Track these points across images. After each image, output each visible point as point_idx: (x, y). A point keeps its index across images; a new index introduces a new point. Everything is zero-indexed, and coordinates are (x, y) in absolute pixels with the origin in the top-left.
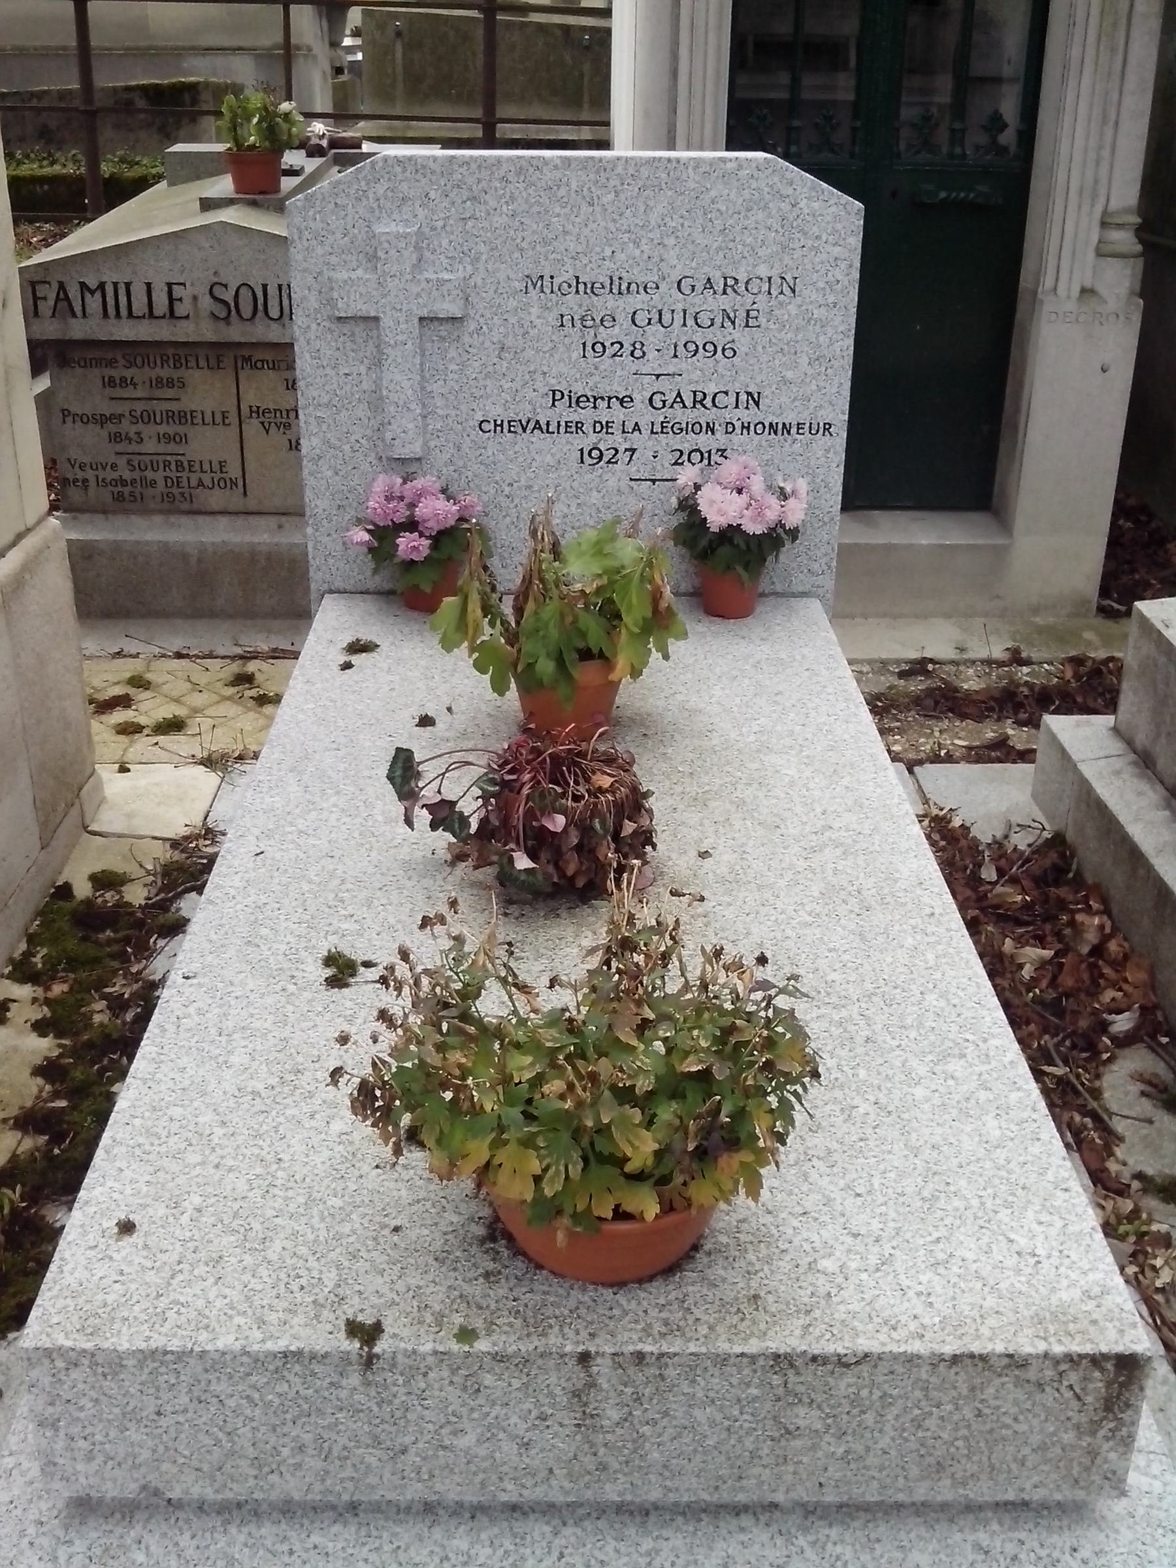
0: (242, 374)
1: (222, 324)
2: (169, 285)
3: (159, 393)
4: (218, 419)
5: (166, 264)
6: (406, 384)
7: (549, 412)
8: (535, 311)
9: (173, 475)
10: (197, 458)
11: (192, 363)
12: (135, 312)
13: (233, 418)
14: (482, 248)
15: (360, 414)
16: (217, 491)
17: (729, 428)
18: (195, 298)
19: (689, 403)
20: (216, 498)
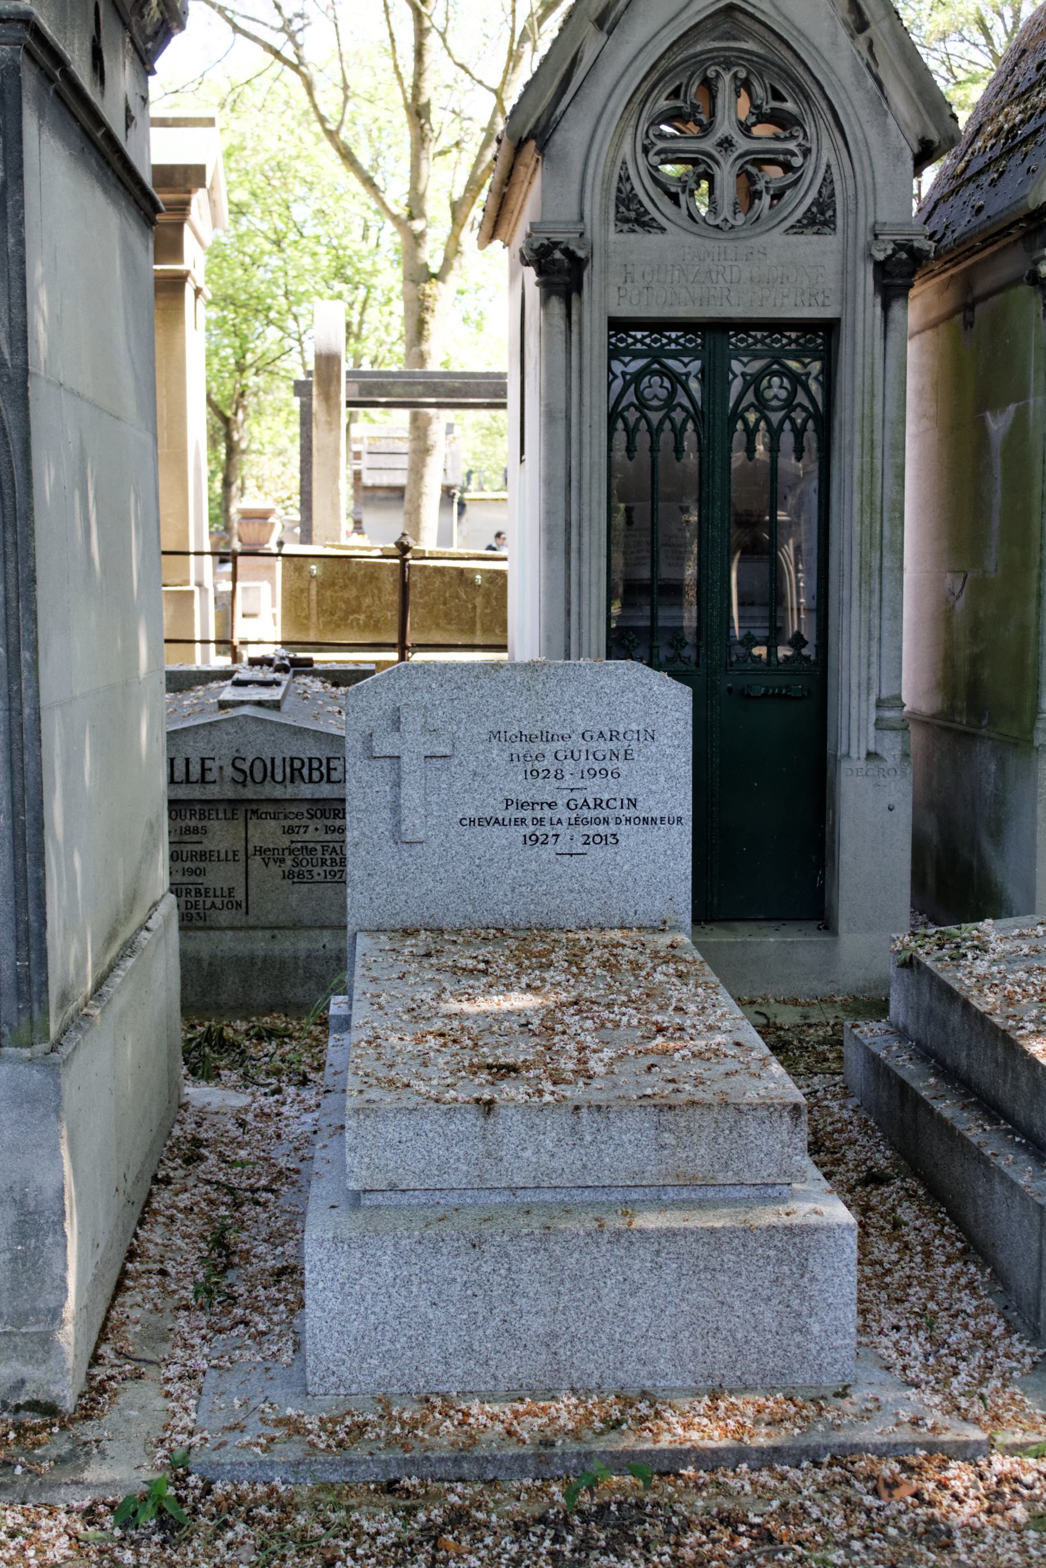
0: (251, 824)
1: (240, 787)
2: (203, 760)
3: (186, 838)
4: (230, 857)
5: (201, 744)
6: (415, 796)
7: (505, 813)
8: (495, 752)
9: (192, 900)
10: (218, 886)
11: (214, 816)
12: (176, 779)
13: (241, 856)
14: (464, 716)
15: (384, 816)
16: (225, 912)
17: (618, 821)
18: (221, 768)
19: (592, 805)
20: (224, 917)
